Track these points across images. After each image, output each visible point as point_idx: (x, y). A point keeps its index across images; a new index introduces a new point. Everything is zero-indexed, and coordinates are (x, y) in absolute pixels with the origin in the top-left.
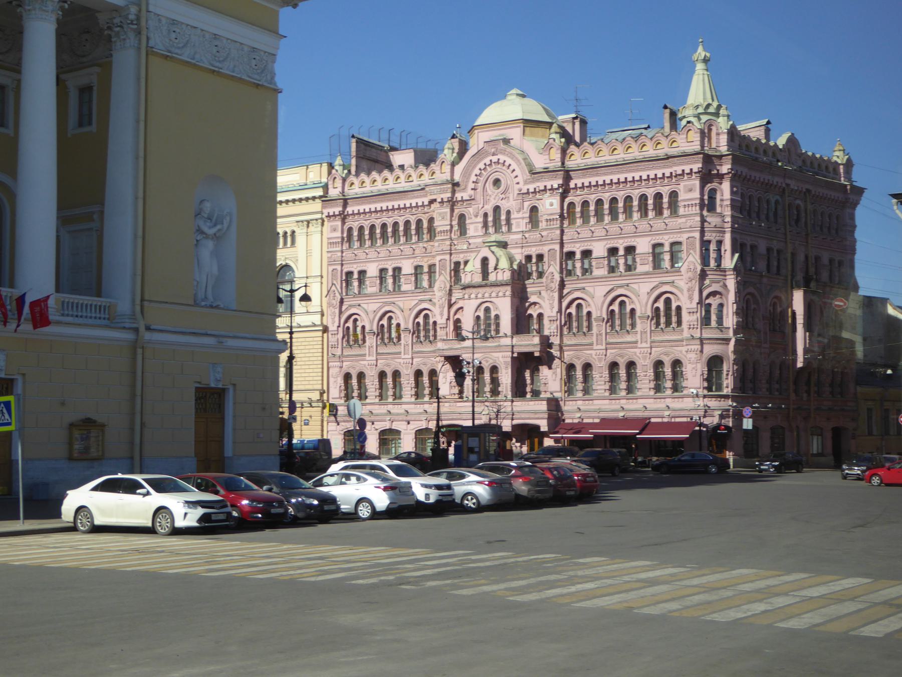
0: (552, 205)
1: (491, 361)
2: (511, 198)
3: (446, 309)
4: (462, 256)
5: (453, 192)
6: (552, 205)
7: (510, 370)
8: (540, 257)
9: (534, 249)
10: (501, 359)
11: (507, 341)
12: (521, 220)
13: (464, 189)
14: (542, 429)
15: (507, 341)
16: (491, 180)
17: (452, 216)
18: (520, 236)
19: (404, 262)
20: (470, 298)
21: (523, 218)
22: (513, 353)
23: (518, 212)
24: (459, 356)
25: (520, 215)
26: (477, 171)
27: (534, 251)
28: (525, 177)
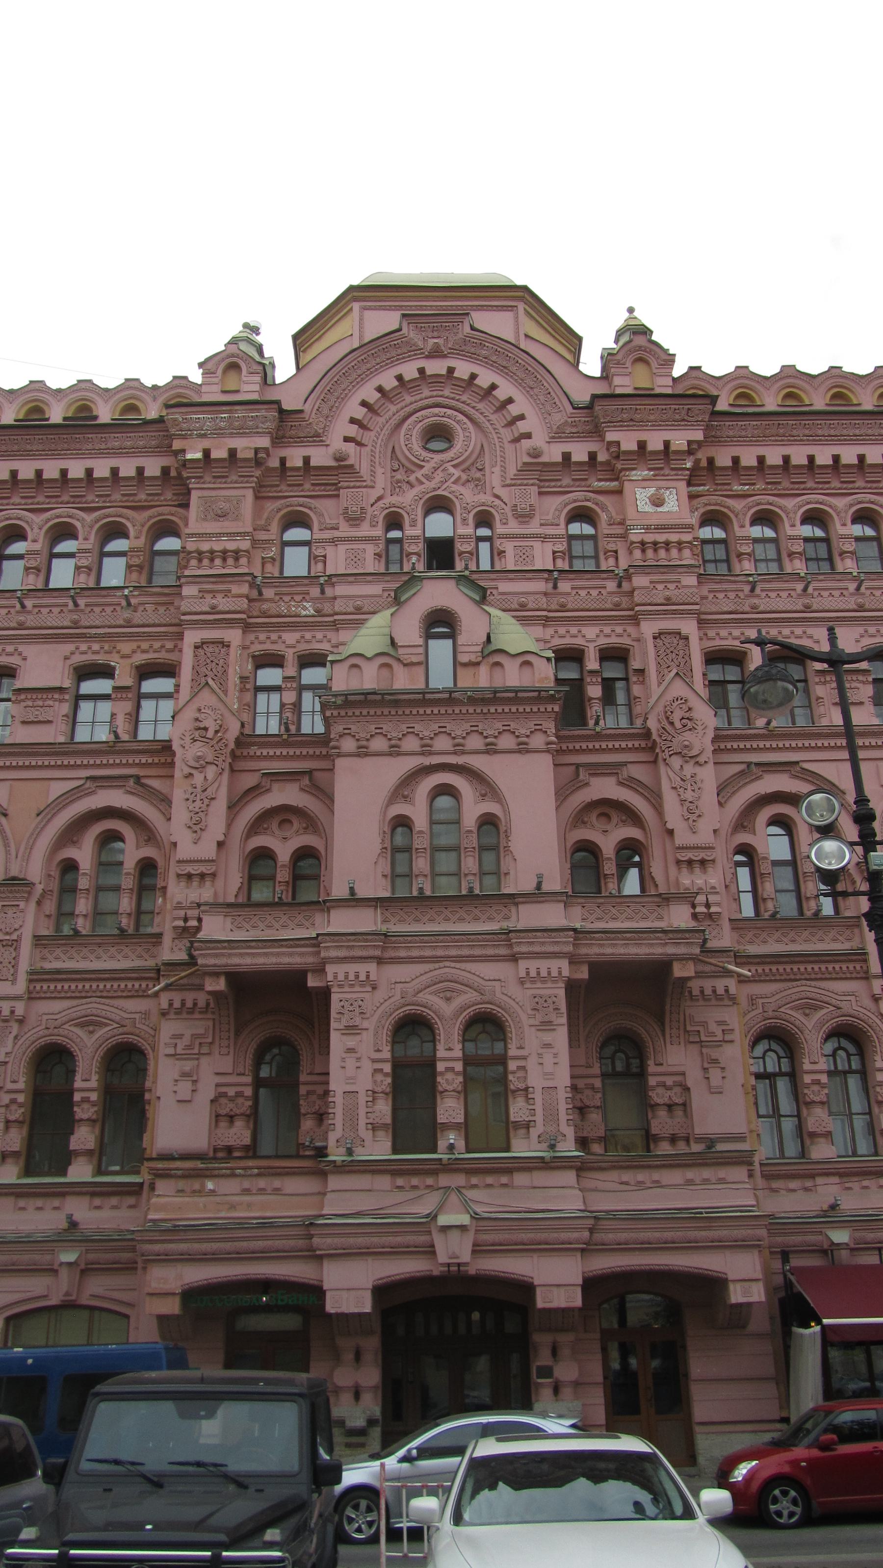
0: (658, 502)
1: (470, 996)
2: (494, 479)
3: (220, 807)
4: (290, 637)
5: (279, 439)
6: (658, 502)
7: (560, 1038)
8: (614, 655)
9: (591, 632)
10: (514, 990)
11: (552, 915)
12: (537, 545)
13: (317, 439)
14: (736, 1295)
15: (552, 915)
16: (414, 429)
17: (257, 512)
18: (540, 586)
19: (28, 650)
20: (363, 753)
21: (544, 538)
22: (574, 960)
23: (524, 517)
24: (299, 976)
25: (534, 528)
26: (388, 380)
27: (591, 638)
28: (558, 419)
